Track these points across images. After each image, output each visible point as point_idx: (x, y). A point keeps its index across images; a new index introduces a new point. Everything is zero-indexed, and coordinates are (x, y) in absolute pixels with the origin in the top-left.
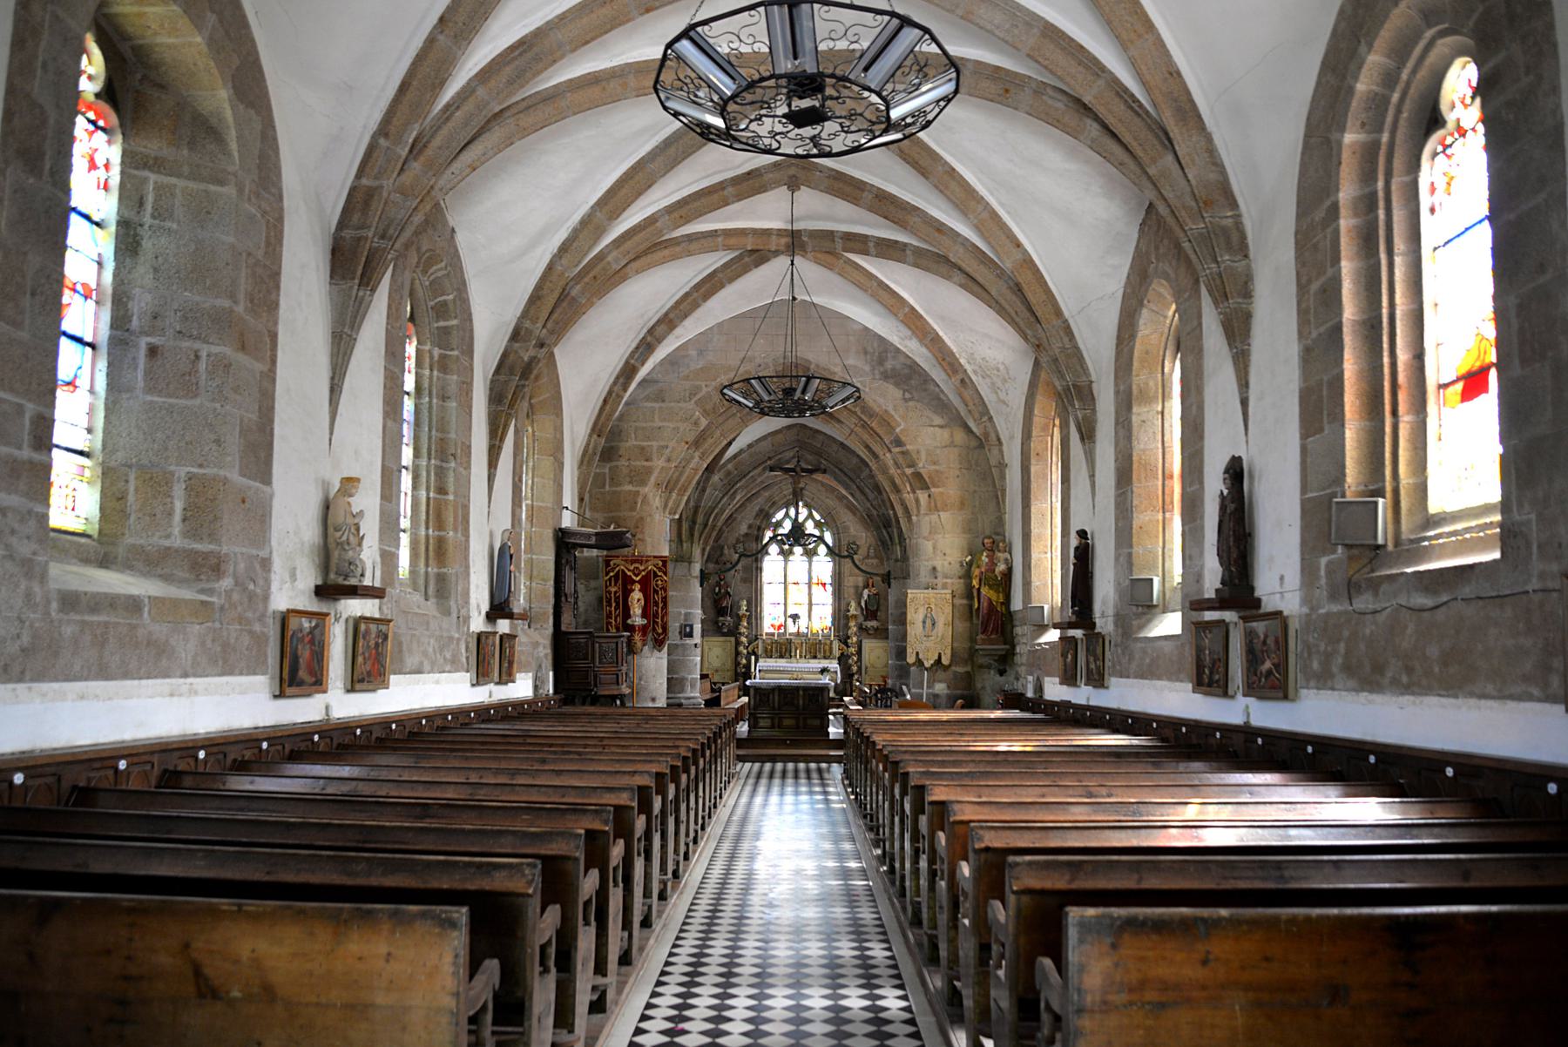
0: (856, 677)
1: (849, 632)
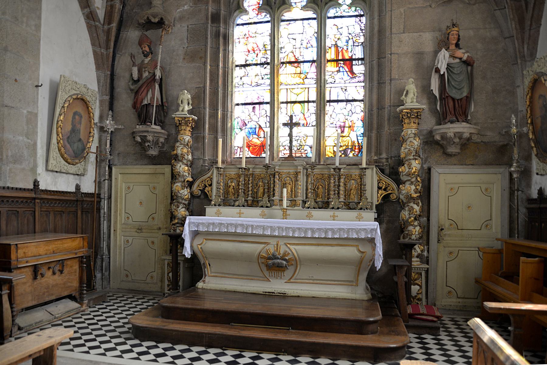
0: (418, 249)
1: (403, 151)
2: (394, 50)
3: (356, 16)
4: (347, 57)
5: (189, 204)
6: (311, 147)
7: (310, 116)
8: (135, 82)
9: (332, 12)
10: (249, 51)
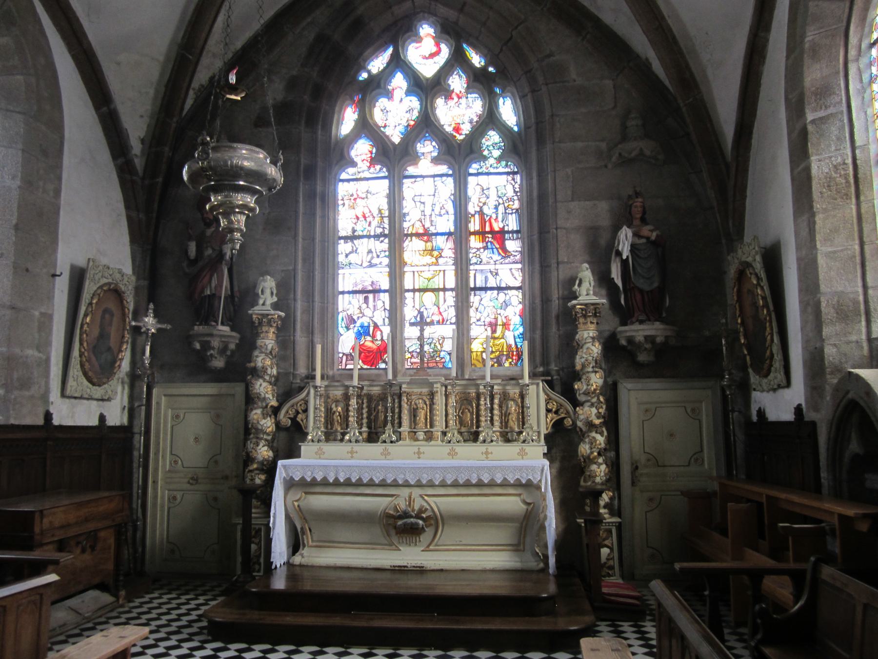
1: (579, 362)
2: (560, 223)
3: (508, 174)
4: (496, 229)
5: (273, 439)
6: (450, 354)
7: (447, 309)
8: (193, 262)
9: (474, 168)
10: (358, 218)
